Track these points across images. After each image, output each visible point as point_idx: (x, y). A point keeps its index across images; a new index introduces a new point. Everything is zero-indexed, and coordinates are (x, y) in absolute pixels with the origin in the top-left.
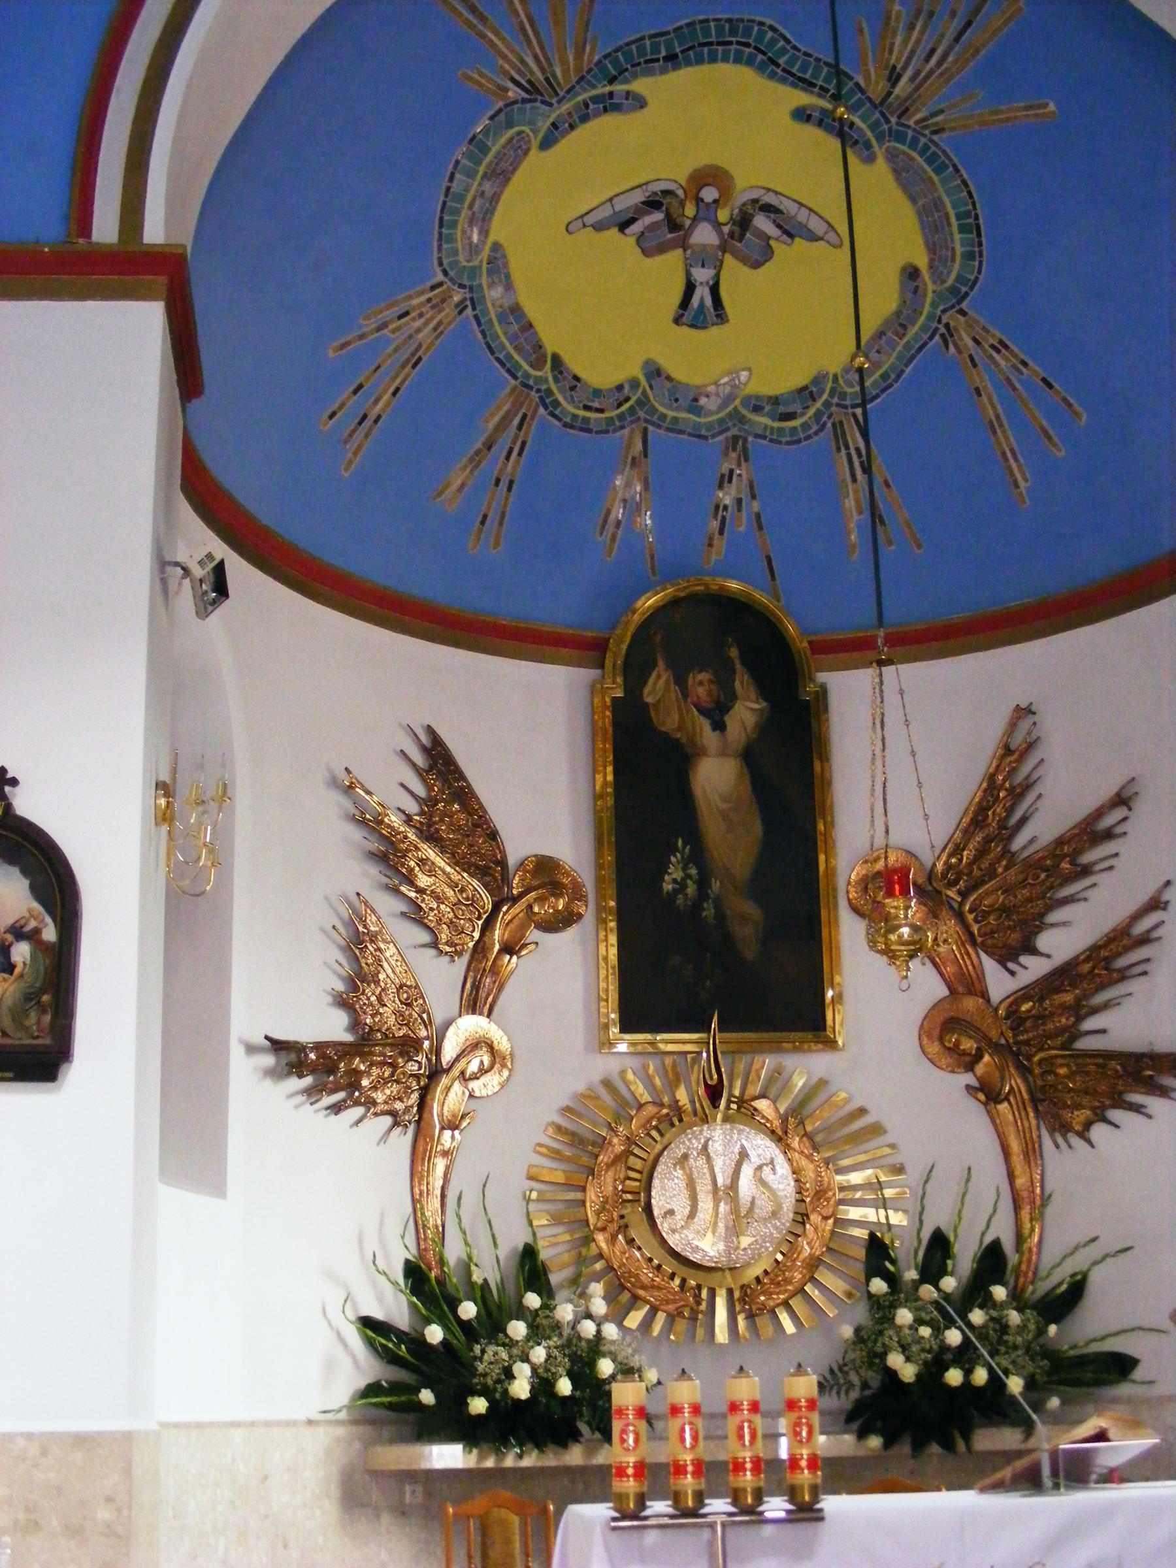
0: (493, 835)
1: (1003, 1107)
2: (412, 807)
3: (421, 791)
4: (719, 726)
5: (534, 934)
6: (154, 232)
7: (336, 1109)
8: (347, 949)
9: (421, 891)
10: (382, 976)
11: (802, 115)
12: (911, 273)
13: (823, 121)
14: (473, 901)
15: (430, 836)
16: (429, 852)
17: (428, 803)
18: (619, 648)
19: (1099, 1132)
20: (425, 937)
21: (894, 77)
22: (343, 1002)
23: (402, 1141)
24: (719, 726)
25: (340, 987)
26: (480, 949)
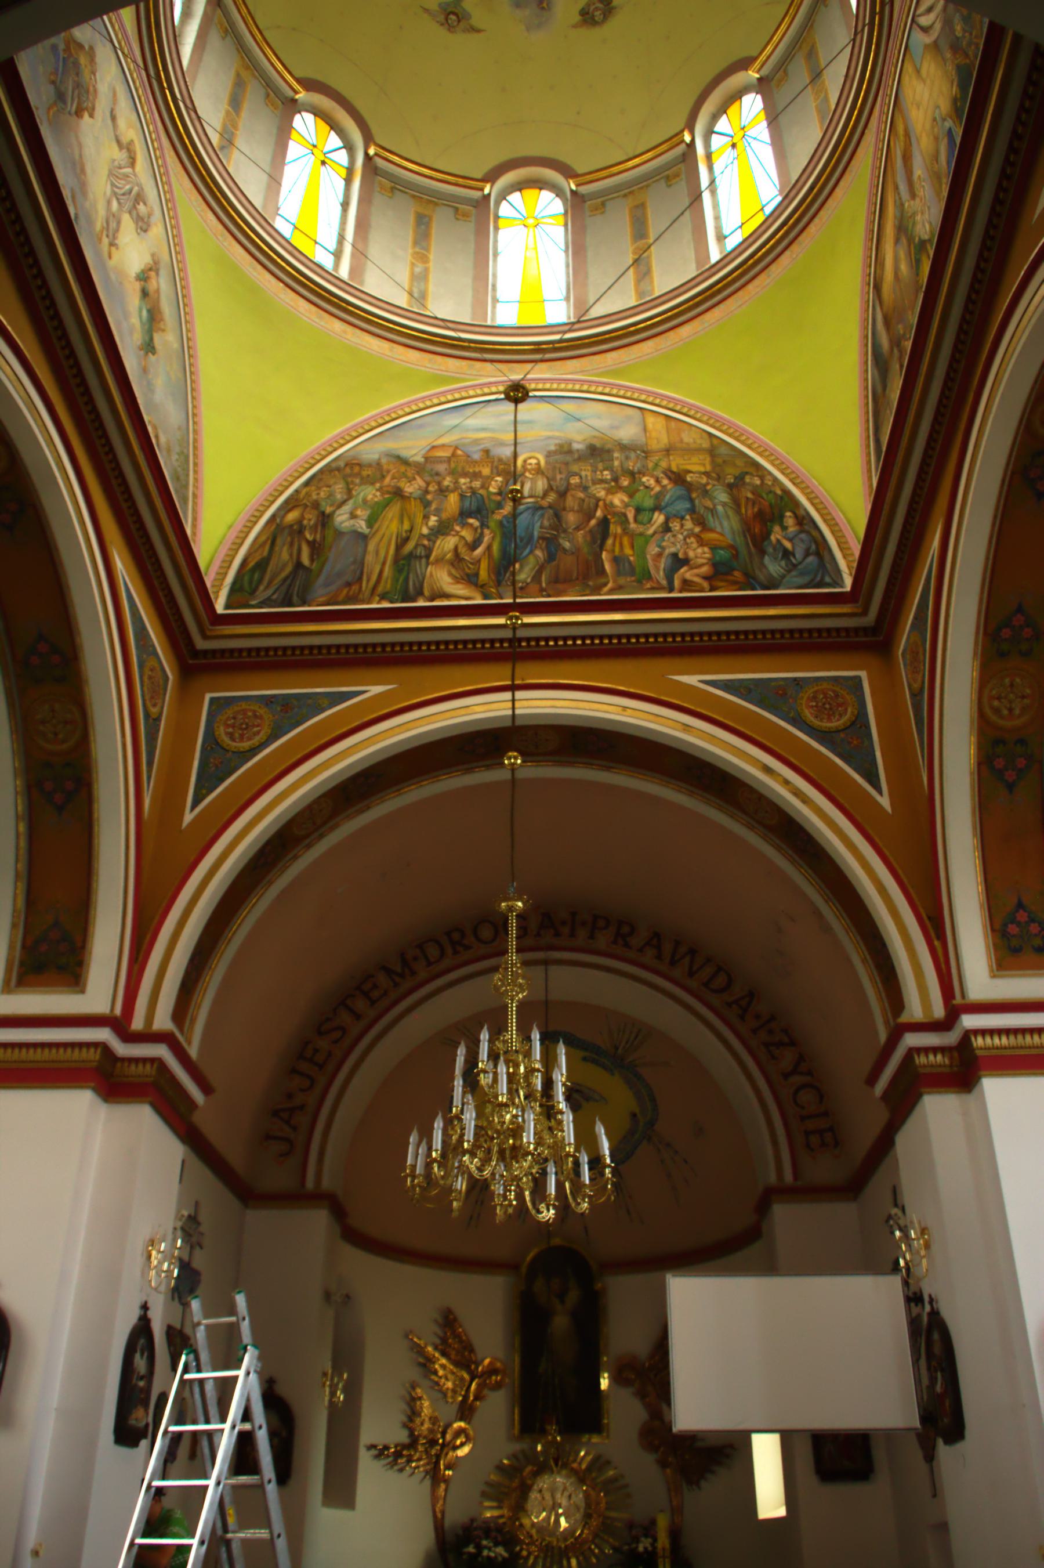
0: (472, 1350)
1: (668, 1471)
2: (438, 1341)
3: (440, 1333)
4: (563, 1302)
5: (486, 1392)
6: (326, 1184)
7: (401, 1470)
8: (408, 1404)
9: (441, 1377)
10: (423, 1414)
11: (585, 1059)
12: (634, 1115)
13: (594, 1061)
14: (462, 1379)
15: (444, 1354)
16: (444, 1361)
17: (444, 1340)
18: (524, 1269)
19: (703, 1483)
20: (440, 1395)
21: (617, 1048)
22: (405, 1425)
23: (428, 1482)
24: (563, 1302)
25: (405, 1419)
26: (466, 1397)
